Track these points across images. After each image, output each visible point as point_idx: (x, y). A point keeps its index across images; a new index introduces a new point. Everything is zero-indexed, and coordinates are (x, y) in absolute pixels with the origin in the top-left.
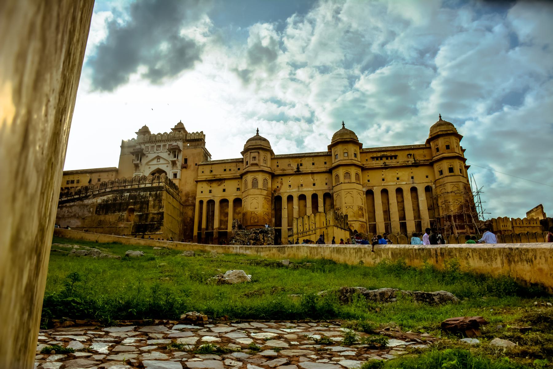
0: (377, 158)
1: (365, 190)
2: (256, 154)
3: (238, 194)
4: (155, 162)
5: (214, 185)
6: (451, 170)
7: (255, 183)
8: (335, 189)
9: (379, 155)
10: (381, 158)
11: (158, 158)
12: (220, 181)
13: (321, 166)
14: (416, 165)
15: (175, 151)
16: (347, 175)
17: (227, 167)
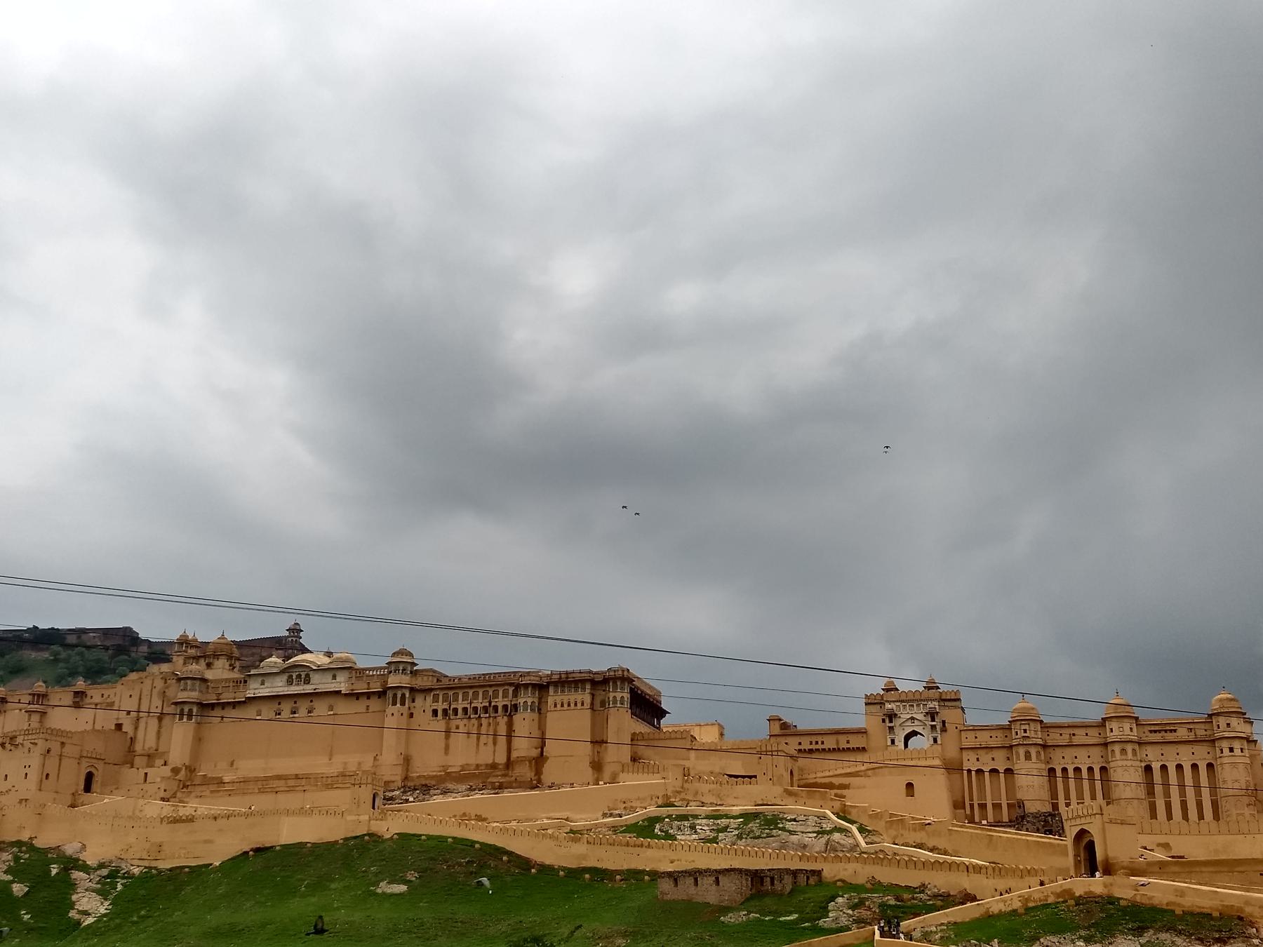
0: (1155, 731)
1: (1143, 764)
2: (1026, 727)
4: (909, 723)
5: (981, 752)
6: (1231, 750)
7: (1028, 756)
8: (1112, 764)
9: (1157, 728)
10: (1160, 731)
11: (912, 718)
13: (1093, 737)
14: (1195, 742)
15: (932, 715)
16: (1123, 751)
17: (994, 734)
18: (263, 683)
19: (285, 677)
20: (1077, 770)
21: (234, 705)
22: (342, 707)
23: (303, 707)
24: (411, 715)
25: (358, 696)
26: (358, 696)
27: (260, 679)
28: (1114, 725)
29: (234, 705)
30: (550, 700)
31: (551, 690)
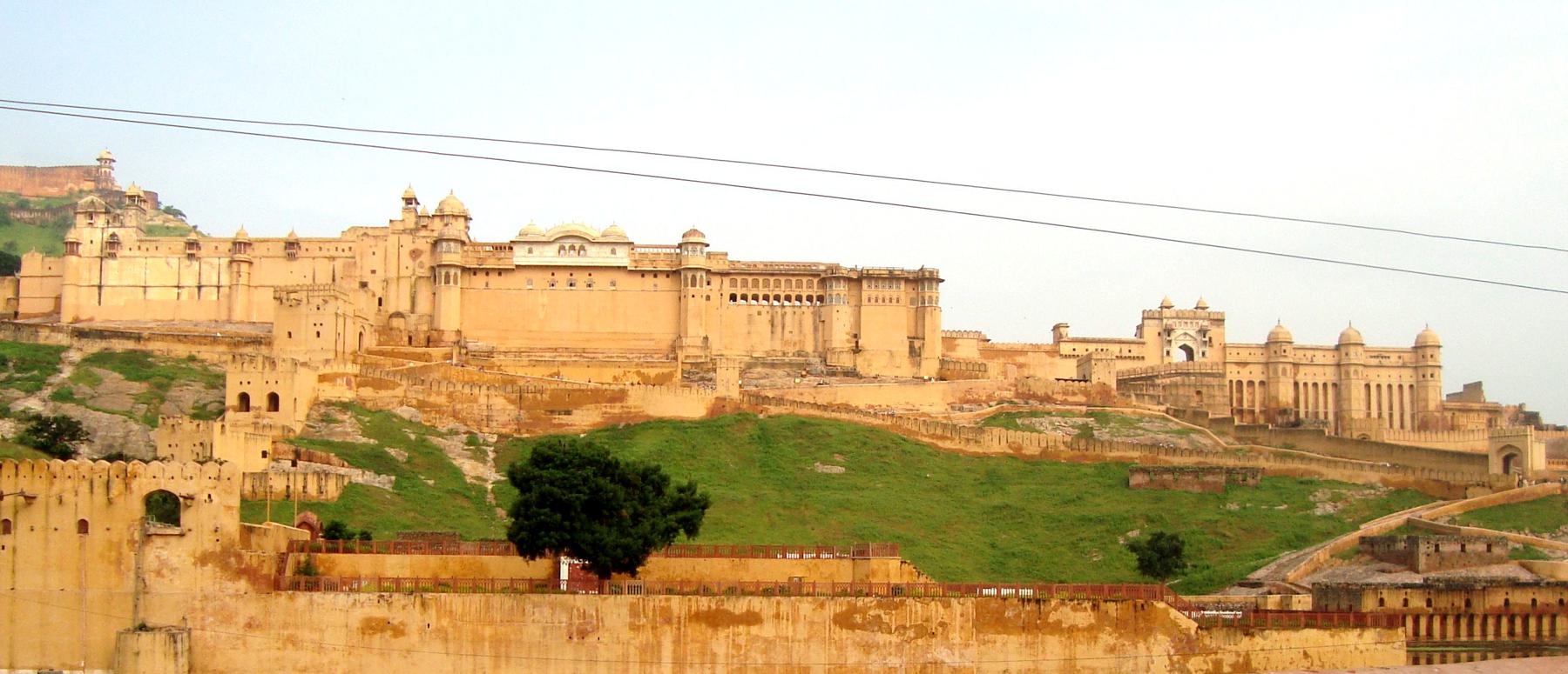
3: (1263, 378)
7: (1284, 371)
12: (1245, 364)
14: (1404, 366)
18: (530, 251)
19: (556, 247)
20: (1315, 385)
21: (500, 272)
22: (623, 280)
23: (582, 278)
24: (708, 298)
25: (643, 274)
26: (643, 274)
27: (527, 247)
28: (1352, 350)
29: (500, 272)
30: (865, 295)
31: (865, 284)
